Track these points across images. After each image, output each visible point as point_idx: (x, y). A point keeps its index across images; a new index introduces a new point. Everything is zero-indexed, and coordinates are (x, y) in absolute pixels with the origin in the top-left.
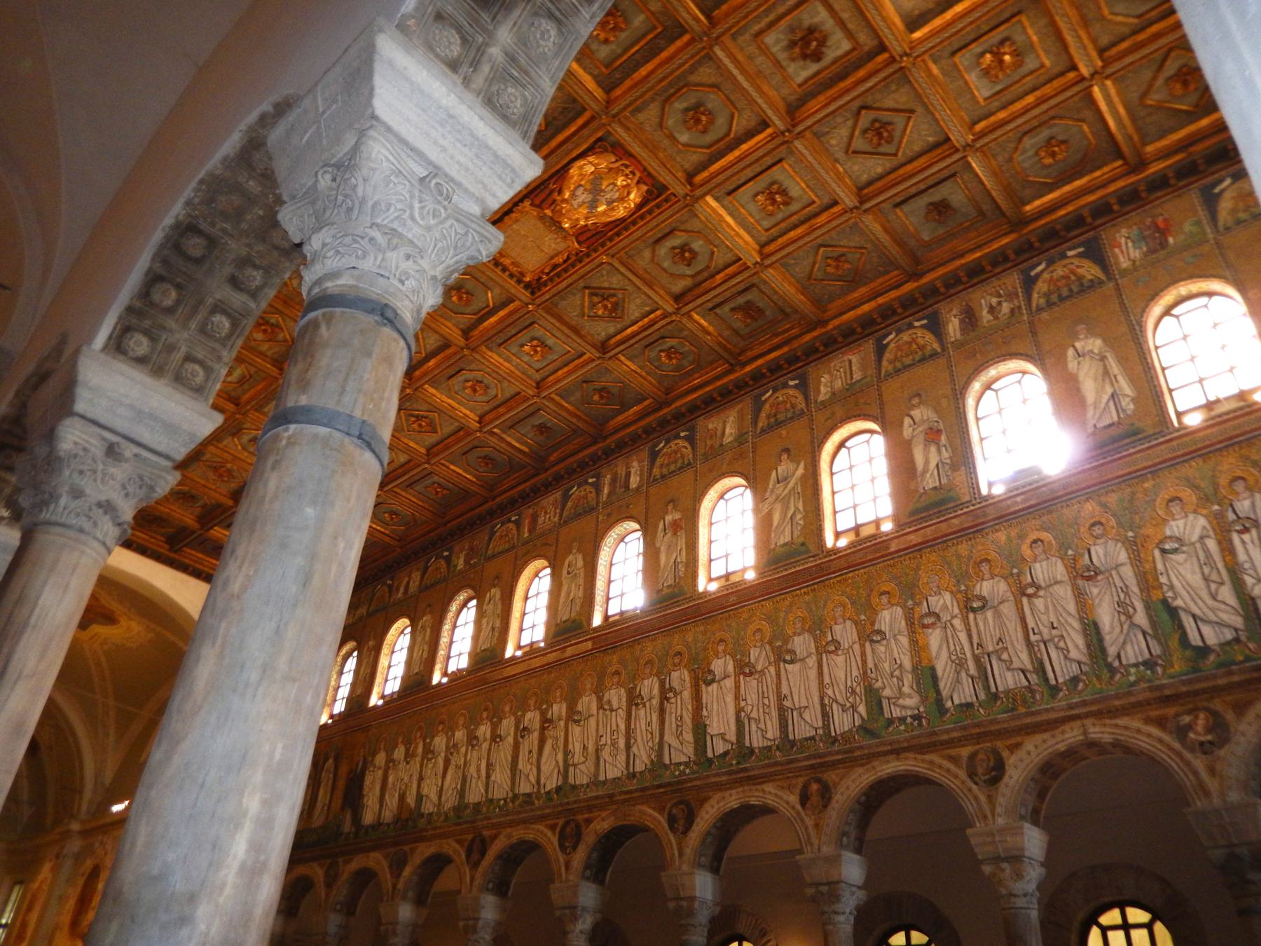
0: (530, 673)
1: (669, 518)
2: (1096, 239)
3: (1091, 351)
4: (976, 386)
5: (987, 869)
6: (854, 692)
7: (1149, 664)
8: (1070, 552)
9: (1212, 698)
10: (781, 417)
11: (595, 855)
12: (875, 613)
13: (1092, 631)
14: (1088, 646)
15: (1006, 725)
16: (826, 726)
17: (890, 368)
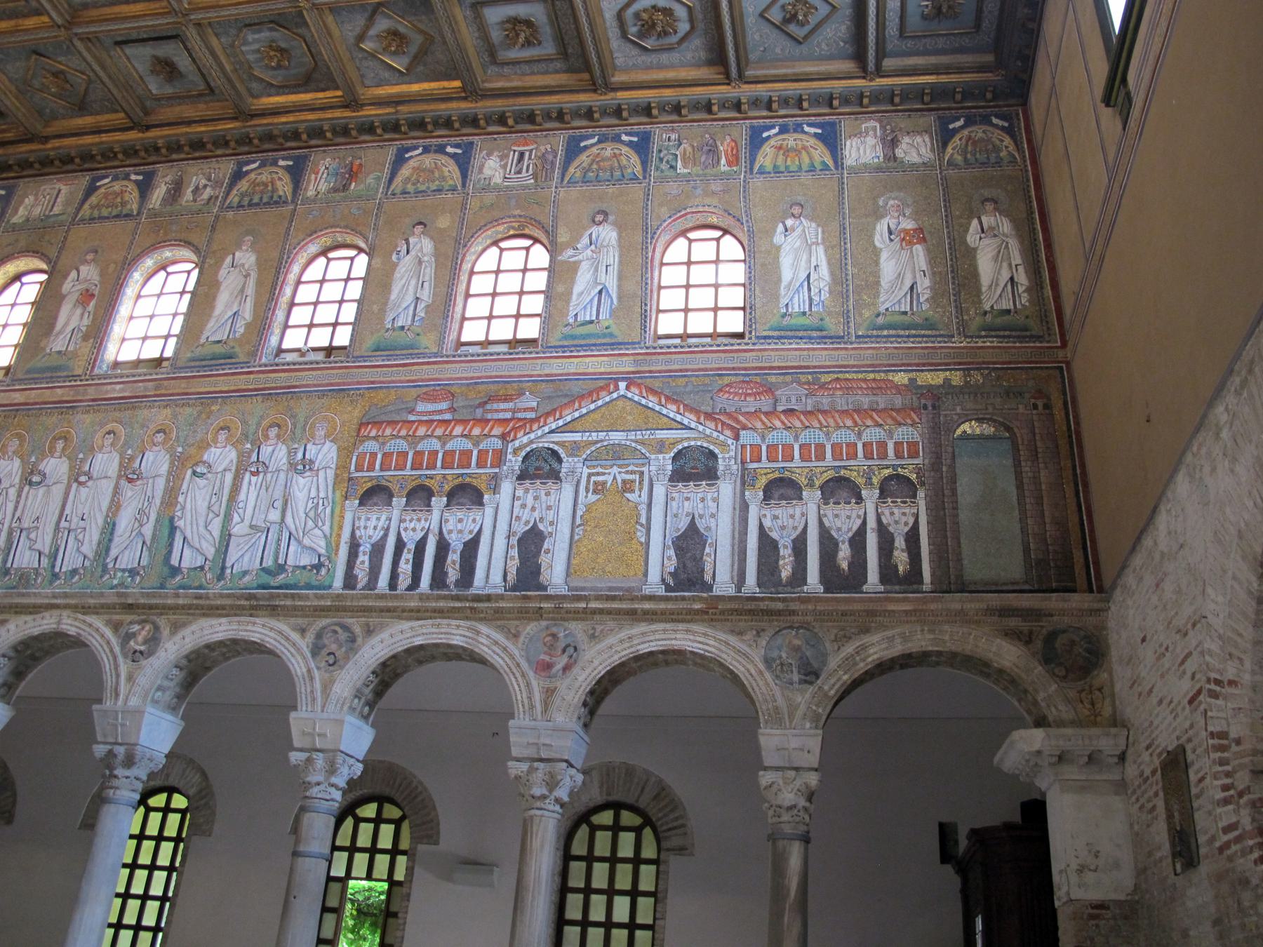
2: (306, 157)
3: (243, 265)
4: (149, 263)
7: (133, 572)
8: (129, 452)
9: (162, 614)
13: (109, 529)
17: (88, 213)
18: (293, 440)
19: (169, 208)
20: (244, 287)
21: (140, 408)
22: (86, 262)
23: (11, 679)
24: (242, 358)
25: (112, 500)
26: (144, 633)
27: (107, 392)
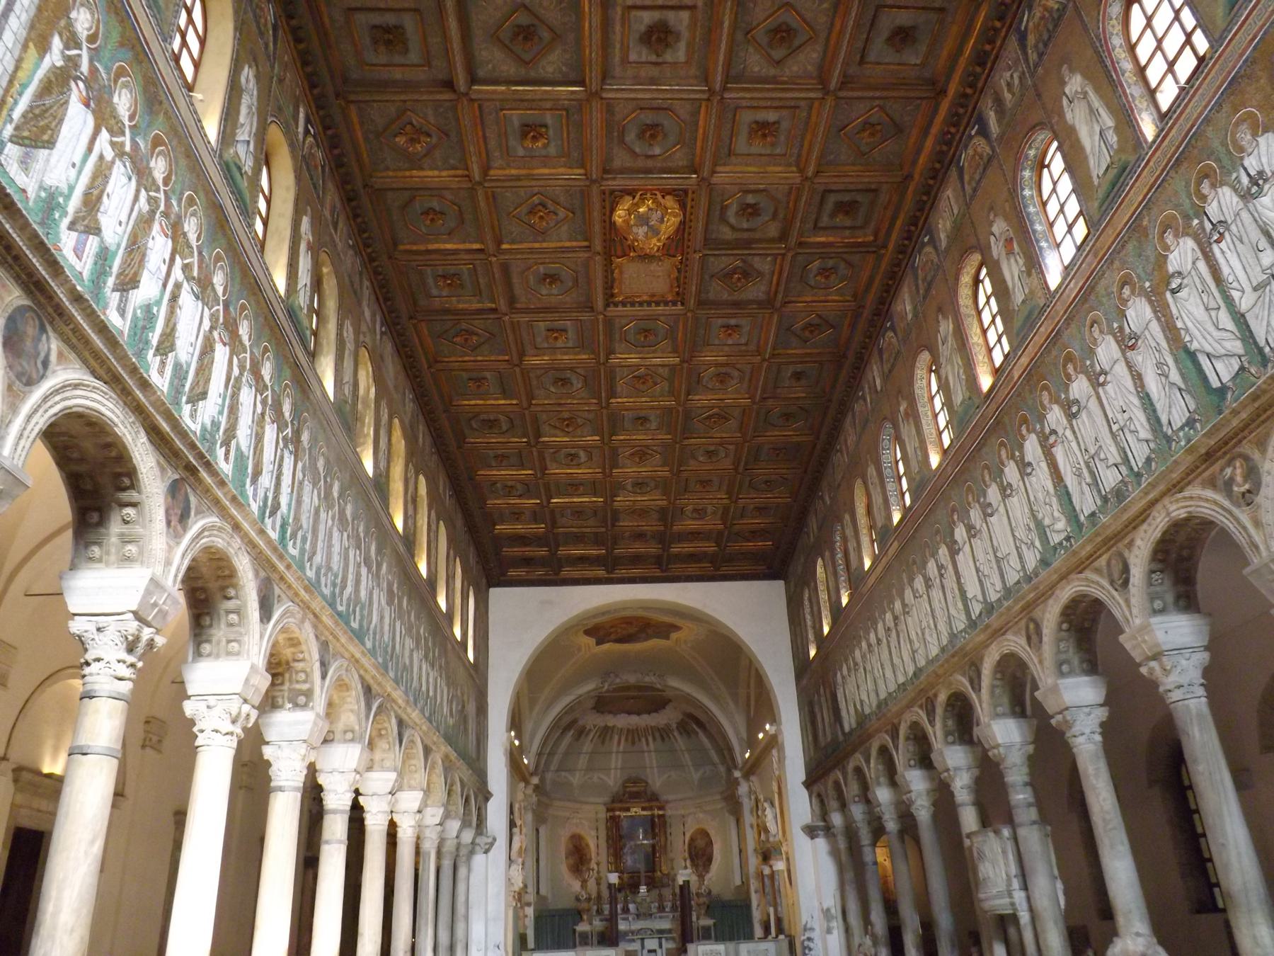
0: (880, 580)
1: (902, 409)
5: (1144, 670)
6: (1030, 529)
7: (1190, 423)
8: (1115, 325)
9: (1240, 441)
10: (929, 278)
11: (950, 723)
12: (1021, 447)
14: (1148, 420)
15: (1113, 527)
16: (1023, 567)
18: (1230, 173)
19: (1005, 122)
20: (1090, 106)
21: (1096, 283)
22: (991, 224)
23: (1182, 589)
24: (1132, 159)
25: (1133, 376)
26: (1239, 471)
27: (1069, 296)
